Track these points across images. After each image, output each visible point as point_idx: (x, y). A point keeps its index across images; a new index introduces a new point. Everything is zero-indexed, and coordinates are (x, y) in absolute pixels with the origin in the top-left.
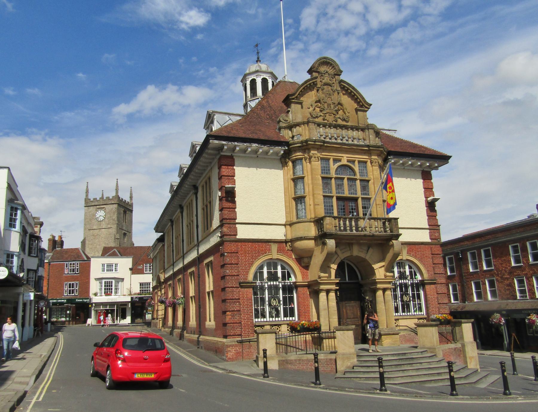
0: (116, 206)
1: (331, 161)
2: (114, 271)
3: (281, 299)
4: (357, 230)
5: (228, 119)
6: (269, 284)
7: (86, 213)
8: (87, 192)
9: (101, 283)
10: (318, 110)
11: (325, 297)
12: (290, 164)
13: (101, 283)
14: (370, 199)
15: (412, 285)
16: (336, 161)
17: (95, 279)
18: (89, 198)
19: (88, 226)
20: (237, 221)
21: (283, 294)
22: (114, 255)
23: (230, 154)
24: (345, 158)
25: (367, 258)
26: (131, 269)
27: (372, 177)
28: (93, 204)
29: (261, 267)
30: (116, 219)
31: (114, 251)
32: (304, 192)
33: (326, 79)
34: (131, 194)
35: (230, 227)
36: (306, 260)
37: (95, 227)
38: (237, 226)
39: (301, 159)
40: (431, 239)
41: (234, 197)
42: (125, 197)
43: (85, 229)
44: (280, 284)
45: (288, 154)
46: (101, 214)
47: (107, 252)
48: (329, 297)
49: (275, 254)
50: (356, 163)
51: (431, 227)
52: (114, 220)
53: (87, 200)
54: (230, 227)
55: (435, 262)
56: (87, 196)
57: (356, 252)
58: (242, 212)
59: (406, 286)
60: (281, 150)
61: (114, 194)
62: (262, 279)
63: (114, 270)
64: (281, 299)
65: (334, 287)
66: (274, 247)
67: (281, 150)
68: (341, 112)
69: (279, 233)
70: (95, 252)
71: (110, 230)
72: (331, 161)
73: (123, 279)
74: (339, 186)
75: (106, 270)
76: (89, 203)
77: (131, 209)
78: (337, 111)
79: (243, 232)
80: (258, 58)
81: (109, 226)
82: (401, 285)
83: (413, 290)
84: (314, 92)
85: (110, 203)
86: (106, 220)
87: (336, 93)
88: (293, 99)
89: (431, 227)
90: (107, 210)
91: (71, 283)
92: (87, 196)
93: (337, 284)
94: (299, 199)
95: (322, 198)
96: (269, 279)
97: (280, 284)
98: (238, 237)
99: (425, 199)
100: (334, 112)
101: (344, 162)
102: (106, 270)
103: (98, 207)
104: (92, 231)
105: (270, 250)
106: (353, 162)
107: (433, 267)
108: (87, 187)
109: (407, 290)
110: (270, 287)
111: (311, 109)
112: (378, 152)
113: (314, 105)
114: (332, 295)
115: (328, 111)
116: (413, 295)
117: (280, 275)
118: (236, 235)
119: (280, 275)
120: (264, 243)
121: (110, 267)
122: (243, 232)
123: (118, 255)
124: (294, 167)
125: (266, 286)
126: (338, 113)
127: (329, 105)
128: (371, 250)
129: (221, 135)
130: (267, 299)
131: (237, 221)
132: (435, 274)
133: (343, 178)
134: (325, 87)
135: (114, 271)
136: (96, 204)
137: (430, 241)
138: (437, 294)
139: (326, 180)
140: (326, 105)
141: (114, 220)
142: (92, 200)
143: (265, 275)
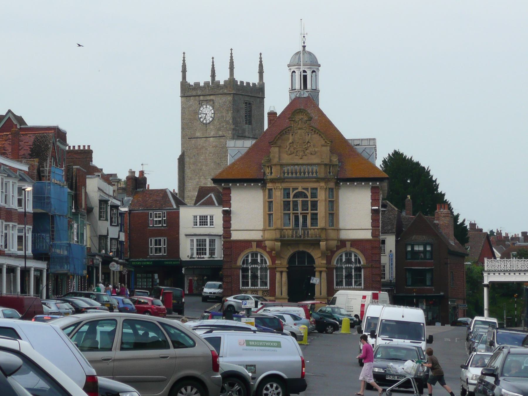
0: (230, 98)
4: (296, 236)
7: (183, 108)
8: (184, 71)
9: (192, 241)
12: (267, 190)
13: (192, 241)
16: (294, 189)
17: (186, 235)
28: (194, 93)
29: (248, 257)
30: (231, 121)
34: (261, 66)
37: (198, 134)
40: (372, 236)
42: (247, 75)
46: (207, 112)
48: (283, 276)
49: (254, 249)
52: (227, 122)
56: (184, 77)
57: (301, 249)
61: (227, 77)
62: (247, 263)
65: (285, 269)
66: (254, 244)
69: (257, 236)
70: (199, 178)
75: (198, 223)
76: (189, 91)
79: (235, 236)
80: (304, 42)
81: (221, 133)
82: (346, 268)
85: (221, 92)
86: (216, 122)
91: (158, 238)
92: (184, 77)
93: (288, 268)
101: (300, 190)
102: (198, 223)
103: (202, 98)
104: (193, 141)
105: (251, 247)
106: (307, 189)
114: (285, 275)
117: (259, 261)
118: (230, 237)
119: (259, 261)
120: (247, 243)
121: (203, 221)
122: (235, 236)
131: (231, 229)
136: (199, 93)
141: (227, 122)
142: (192, 83)
143: (250, 261)
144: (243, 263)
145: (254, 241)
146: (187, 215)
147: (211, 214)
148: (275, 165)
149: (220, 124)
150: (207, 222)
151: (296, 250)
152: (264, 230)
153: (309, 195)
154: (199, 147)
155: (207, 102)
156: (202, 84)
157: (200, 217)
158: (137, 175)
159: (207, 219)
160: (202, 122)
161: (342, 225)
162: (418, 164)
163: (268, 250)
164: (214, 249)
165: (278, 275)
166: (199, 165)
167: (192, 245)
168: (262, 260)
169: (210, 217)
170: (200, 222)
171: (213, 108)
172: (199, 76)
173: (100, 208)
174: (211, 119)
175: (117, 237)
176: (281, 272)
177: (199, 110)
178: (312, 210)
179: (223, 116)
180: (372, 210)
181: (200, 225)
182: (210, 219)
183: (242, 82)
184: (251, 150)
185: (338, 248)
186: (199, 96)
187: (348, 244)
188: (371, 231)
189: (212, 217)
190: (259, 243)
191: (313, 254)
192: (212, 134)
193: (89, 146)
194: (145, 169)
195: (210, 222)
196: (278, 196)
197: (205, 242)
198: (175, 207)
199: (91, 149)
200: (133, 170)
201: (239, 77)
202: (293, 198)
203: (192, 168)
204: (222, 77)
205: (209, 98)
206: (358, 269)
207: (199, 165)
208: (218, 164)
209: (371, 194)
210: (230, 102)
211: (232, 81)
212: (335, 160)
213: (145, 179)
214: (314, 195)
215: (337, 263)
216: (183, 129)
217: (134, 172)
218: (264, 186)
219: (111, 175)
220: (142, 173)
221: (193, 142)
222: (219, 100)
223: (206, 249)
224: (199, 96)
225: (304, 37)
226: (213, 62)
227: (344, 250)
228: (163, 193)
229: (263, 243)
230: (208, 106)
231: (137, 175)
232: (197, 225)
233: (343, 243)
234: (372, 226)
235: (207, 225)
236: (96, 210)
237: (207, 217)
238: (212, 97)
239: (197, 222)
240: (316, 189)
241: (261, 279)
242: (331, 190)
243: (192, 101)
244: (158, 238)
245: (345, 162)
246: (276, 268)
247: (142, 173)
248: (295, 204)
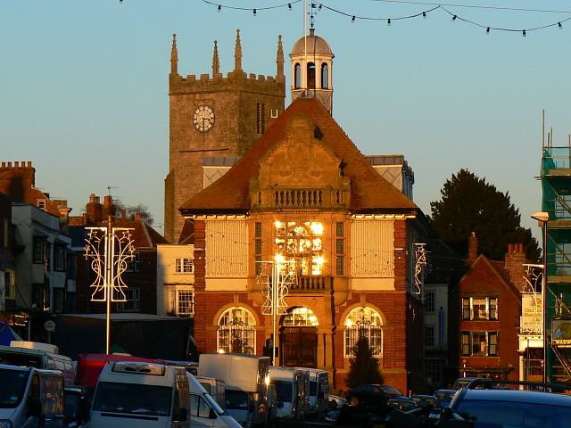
7: (172, 111)
28: (188, 90)
29: (227, 314)
37: (192, 147)
43: (172, 151)
46: (203, 116)
52: (232, 130)
56: (174, 68)
61: (232, 68)
66: (236, 298)
69: (241, 285)
75: (182, 269)
76: (180, 87)
77: (280, 93)
79: (212, 286)
81: (223, 145)
83: (372, 334)
85: (223, 88)
86: (216, 130)
92: (174, 68)
102: (182, 269)
104: (186, 156)
108: (174, 46)
122: (212, 286)
141: (232, 130)
142: (185, 77)
144: (222, 323)
145: (236, 293)
154: (194, 164)
156: (198, 78)
158: (102, 202)
160: (198, 130)
161: (354, 271)
162: (493, 188)
163: (255, 305)
166: (194, 188)
170: (185, 267)
171: (213, 112)
172: (195, 66)
173: (34, 248)
174: (210, 126)
175: (62, 285)
179: (226, 123)
180: (395, 251)
181: (185, 271)
184: (230, 173)
186: (196, 93)
187: (363, 299)
192: (211, 147)
193: (30, 163)
198: (151, 246)
199: (33, 166)
201: (249, 68)
203: (184, 192)
205: (207, 96)
207: (194, 188)
210: (236, 103)
211: (238, 75)
212: (347, 184)
216: (172, 139)
217: (98, 198)
219: (59, 202)
221: (186, 157)
222: (223, 100)
225: (312, 17)
226: (216, 47)
230: (206, 108)
232: (180, 271)
236: (29, 251)
238: (211, 95)
239: (180, 267)
245: (359, 186)
247: (109, 199)
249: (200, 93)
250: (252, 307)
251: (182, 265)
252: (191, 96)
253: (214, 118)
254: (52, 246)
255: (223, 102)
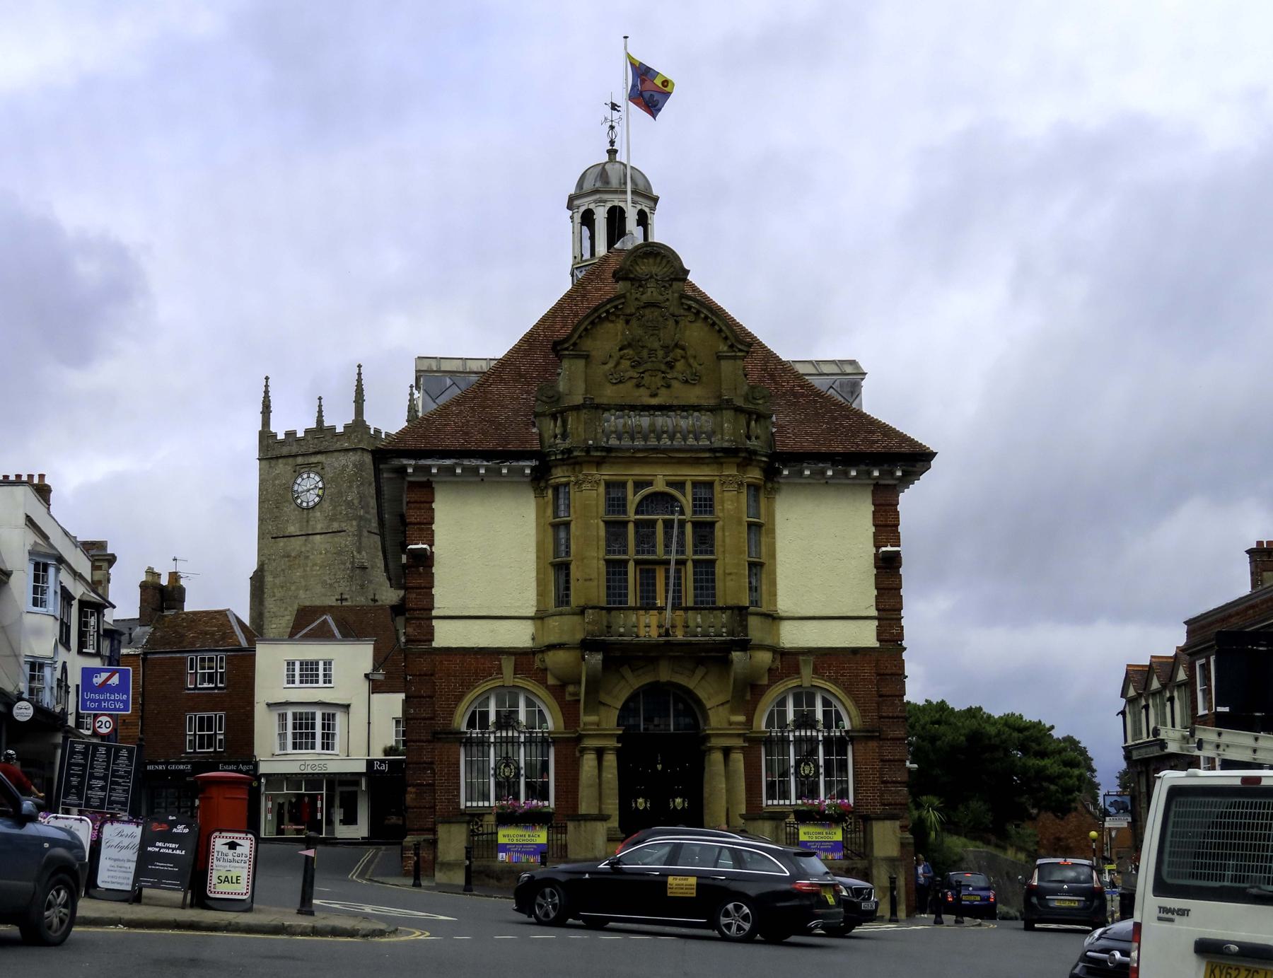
1: (630, 487)
2: (321, 684)
3: (522, 764)
5: (449, 382)
6: (498, 735)
9: (283, 717)
10: (626, 364)
11: (595, 763)
12: (550, 492)
13: (283, 717)
14: (713, 562)
15: (828, 742)
16: (639, 485)
17: (269, 705)
18: (273, 429)
19: (270, 527)
20: (434, 613)
21: (825, 755)
22: (322, 635)
23: (425, 479)
24: (660, 479)
25: (691, 685)
26: (367, 676)
27: (721, 515)
28: (285, 451)
30: (356, 502)
31: (325, 622)
32: (568, 553)
33: (651, 293)
35: (420, 626)
36: (571, 689)
37: (292, 529)
38: (435, 622)
39: (567, 484)
41: (432, 566)
44: (522, 736)
45: (542, 472)
46: (309, 487)
47: (307, 624)
48: (605, 764)
50: (689, 487)
51: (884, 615)
53: (266, 436)
54: (420, 626)
55: (885, 691)
56: (266, 422)
57: (665, 674)
58: (445, 597)
59: (813, 741)
60: (527, 466)
61: (350, 418)
63: (321, 678)
64: (522, 764)
65: (613, 743)
66: (508, 665)
67: (527, 466)
68: (680, 365)
69: (519, 636)
71: (337, 539)
72: (630, 487)
73: (348, 706)
74: (640, 540)
75: (297, 679)
76: (273, 450)
78: (670, 366)
79: (446, 635)
80: (612, 143)
81: (335, 526)
82: (799, 741)
84: (620, 325)
85: (338, 446)
86: (326, 505)
87: (671, 323)
88: (567, 349)
89: (884, 615)
90: (329, 474)
91: (205, 715)
92: (266, 422)
93: (619, 738)
94: (562, 568)
95: (602, 563)
96: (500, 725)
97: (522, 736)
98: (435, 644)
99: (874, 550)
100: (663, 367)
101: (660, 486)
102: (297, 679)
103: (300, 460)
104: (281, 543)
105: (500, 670)
106: (680, 485)
107: (878, 703)
108: (266, 392)
109: (814, 752)
110: (501, 742)
111: (611, 365)
112: (739, 460)
113: (617, 355)
114: (611, 760)
115: (649, 366)
116: (828, 763)
121: (309, 672)
122: (446, 635)
123: (334, 635)
124: (556, 497)
125: (492, 739)
126: (672, 367)
127: (652, 351)
128: (700, 672)
129: (402, 446)
130: (492, 765)
131: (434, 613)
132: (881, 717)
133: (654, 522)
134: (647, 311)
135: (321, 684)
136: (295, 449)
137: (877, 645)
138: (882, 761)
139: (615, 529)
140: (645, 353)
141: (349, 504)
142: (281, 436)
144: (471, 724)
146: (273, 666)
147: (327, 657)
148: (577, 408)
149: (335, 508)
150: (317, 675)
151: (647, 679)
152: (540, 617)
153: (687, 501)
155: (309, 467)
156: (300, 434)
157: (301, 664)
158: (164, 581)
159: (317, 670)
160: (299, 506)
161: (784, 604)
163: (551, 681)
164: (333, 735)
165: (589, 761)
167: (283, 726)
168: (530, 715)
169: (325, 664)
170: (301, 676)
172: (292, 419)
174: (317, 499)
176: (600, 752)
177: (295, 482)
178: (695, 553)
181: (301, 682)
182: (325, 670)
183: (377, 431)
185: (774, 675)
186: (296, 456)
188: (876, 623)
189: (328, 664)
190: (523, 658)
191: (701, 694)
193: (42, 476)
194: (181, 569)
195: (325, 675)
196: (588, 499)
197: (313, 719)
198: (244, 644)
199: (47, 482)
200: (156, 570)
202: (637, 513)
203: (278, 595)
204: (339, 419)
205: (314, 459)
206: (836, 746)
208: (331, 585)
209: (872, 508)
213: (182, 591)
214: (705, 503)
215: (770, 723)
216: (261, 520)
218: (539, 480)
220: (174, 576)
223: (313, 735)
224: (296, 456)
225: (612, 127)
227: (793, 683)
228: (220, 618)
229: (538, 657)
231: (164, 581)
232: (293, 682)
233: (789, 660)
234: (877, 609)
235: (317, 682)
237: (317, 663)
238: (319, 458)
239: (293, 676)
240: (710, 485)
241: (527, 777)
242: (754, 489)
243: (282, 468)
244: (205, 715)
246: (579, 738)
247: (174, 576)
248: (645, 528)
249: (303, 455)
250: (547, 687)
251: (297, 672)
252: (290, 460)
253: (323, 489)
254: (75, 604)
255: (336, 465)
